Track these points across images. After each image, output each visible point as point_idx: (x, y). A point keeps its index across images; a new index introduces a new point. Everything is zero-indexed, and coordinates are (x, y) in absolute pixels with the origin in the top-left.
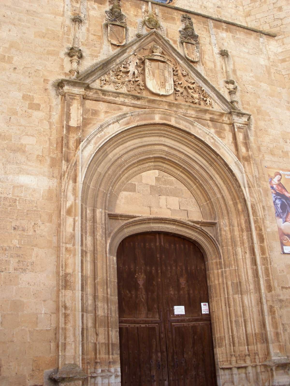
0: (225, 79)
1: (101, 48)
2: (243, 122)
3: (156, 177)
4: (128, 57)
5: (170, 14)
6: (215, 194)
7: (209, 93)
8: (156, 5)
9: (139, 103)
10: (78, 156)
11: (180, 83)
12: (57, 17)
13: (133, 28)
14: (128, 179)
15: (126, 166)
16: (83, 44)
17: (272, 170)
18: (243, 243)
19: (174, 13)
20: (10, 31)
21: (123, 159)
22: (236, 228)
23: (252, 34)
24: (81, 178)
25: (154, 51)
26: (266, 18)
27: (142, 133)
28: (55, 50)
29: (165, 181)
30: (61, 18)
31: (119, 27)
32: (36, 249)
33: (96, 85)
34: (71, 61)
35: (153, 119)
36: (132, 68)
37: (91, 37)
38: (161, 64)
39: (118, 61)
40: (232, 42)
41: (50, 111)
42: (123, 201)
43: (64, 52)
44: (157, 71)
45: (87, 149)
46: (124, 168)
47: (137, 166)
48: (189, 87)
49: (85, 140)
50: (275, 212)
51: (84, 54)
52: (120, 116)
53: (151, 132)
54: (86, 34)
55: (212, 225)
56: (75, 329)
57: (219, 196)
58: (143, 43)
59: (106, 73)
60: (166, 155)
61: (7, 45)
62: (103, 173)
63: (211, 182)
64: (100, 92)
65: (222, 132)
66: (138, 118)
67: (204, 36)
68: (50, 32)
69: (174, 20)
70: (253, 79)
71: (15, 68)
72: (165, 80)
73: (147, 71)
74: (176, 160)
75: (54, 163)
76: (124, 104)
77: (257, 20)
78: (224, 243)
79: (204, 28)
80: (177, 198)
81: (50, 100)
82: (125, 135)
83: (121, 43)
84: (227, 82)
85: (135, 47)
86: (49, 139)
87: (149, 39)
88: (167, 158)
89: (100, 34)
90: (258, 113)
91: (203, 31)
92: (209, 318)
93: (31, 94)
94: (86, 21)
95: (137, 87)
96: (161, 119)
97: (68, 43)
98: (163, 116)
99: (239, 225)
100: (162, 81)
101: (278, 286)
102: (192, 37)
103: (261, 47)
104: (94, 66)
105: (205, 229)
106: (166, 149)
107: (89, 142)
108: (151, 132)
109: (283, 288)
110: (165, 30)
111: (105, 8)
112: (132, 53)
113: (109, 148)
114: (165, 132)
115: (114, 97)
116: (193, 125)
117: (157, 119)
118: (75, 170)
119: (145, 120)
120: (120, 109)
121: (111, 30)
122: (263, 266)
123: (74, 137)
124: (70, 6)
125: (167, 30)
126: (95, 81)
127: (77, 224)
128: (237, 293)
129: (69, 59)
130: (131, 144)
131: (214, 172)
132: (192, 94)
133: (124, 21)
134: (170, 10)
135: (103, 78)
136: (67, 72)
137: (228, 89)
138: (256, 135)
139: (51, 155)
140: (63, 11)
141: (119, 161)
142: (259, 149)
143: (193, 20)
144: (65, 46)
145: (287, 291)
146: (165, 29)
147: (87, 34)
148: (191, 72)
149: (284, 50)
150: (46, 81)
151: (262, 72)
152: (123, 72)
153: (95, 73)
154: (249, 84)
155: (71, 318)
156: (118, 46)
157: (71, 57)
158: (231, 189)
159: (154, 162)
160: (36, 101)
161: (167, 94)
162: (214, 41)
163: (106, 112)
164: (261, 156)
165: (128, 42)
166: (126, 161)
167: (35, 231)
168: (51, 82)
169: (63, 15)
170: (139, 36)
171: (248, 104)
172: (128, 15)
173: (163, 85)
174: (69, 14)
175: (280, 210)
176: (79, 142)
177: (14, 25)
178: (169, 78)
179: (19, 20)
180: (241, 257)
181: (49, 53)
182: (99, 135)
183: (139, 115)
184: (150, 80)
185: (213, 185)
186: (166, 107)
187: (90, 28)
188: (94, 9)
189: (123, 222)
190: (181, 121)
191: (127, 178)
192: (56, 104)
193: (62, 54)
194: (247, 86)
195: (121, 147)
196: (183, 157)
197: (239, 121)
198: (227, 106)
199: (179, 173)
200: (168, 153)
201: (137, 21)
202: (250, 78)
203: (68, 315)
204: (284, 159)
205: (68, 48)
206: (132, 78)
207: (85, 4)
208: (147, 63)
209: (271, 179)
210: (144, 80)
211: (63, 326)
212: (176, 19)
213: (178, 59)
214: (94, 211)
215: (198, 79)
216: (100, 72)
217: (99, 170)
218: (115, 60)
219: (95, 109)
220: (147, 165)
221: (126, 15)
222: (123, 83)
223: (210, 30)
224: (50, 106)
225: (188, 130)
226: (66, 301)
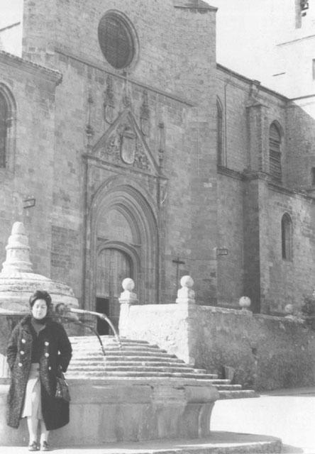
18: (152, 260)
36: (117, 143)
55: (140, 247)
76: (111, 170)
105: (136, 249)
197: (163, 183)
210: (121, 153)
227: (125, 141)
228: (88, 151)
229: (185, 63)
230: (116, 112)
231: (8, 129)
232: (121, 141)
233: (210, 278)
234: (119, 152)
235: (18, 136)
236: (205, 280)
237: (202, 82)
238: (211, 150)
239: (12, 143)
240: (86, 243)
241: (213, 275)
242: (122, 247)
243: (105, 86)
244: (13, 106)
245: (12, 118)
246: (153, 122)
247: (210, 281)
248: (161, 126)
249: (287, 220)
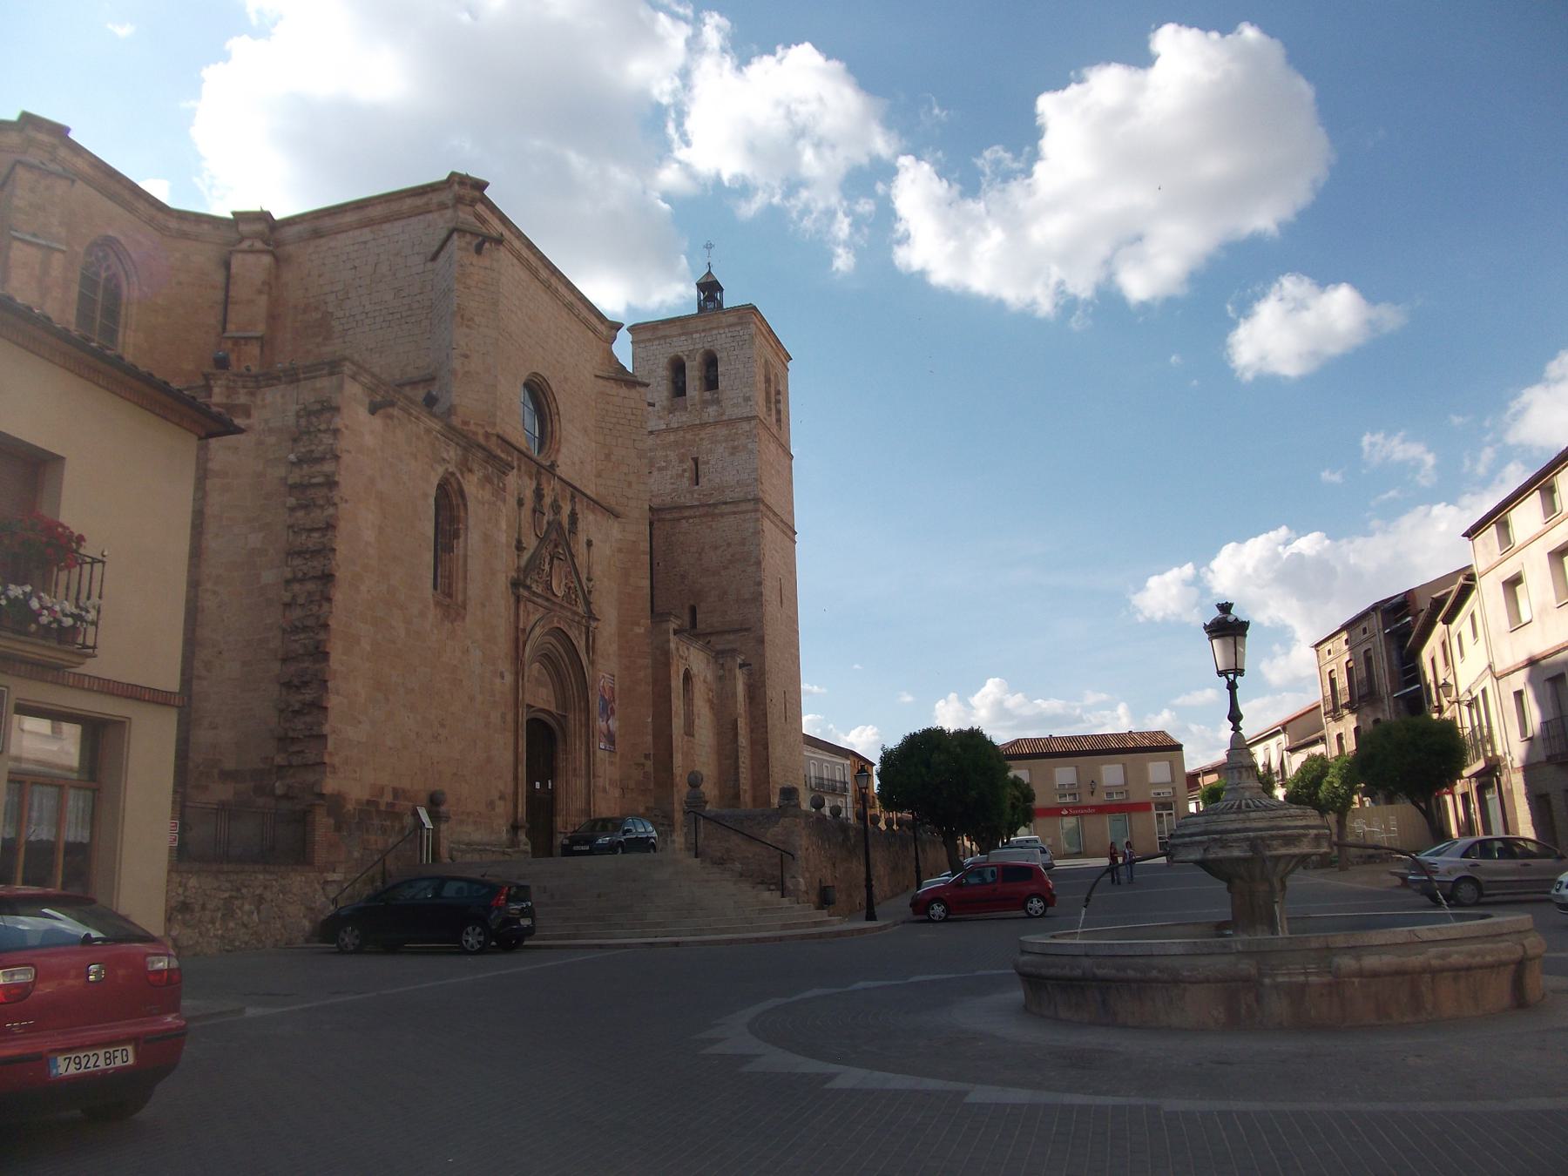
18: (580, 736)
22: (577, 722)
24: (526, 678)
36: (547, 567)
55: (565, 716)
72: (561, 582)
92: (552, 792)
99: (580, 720)
196: (557, 654)
197: (594, 624)
200: (552, 652)
209: (600, 681)
227: (555, 561)
228: (518, 576)
229: (608, 456)
230: (546, 518)
231: (455, 541)
234: (549, 579)
235: (469, 553)
236: (638, 764)
237: (630, 484)
239: (461, 562)
240: (518, 711)
241: (647, 756)
242: (546, 716)
243: (534, 486)
244: (462, 507)
245: (461, 526)
246: (582, 538)
247: (643, 765)
248: (589, 544)
249: (687, 677)
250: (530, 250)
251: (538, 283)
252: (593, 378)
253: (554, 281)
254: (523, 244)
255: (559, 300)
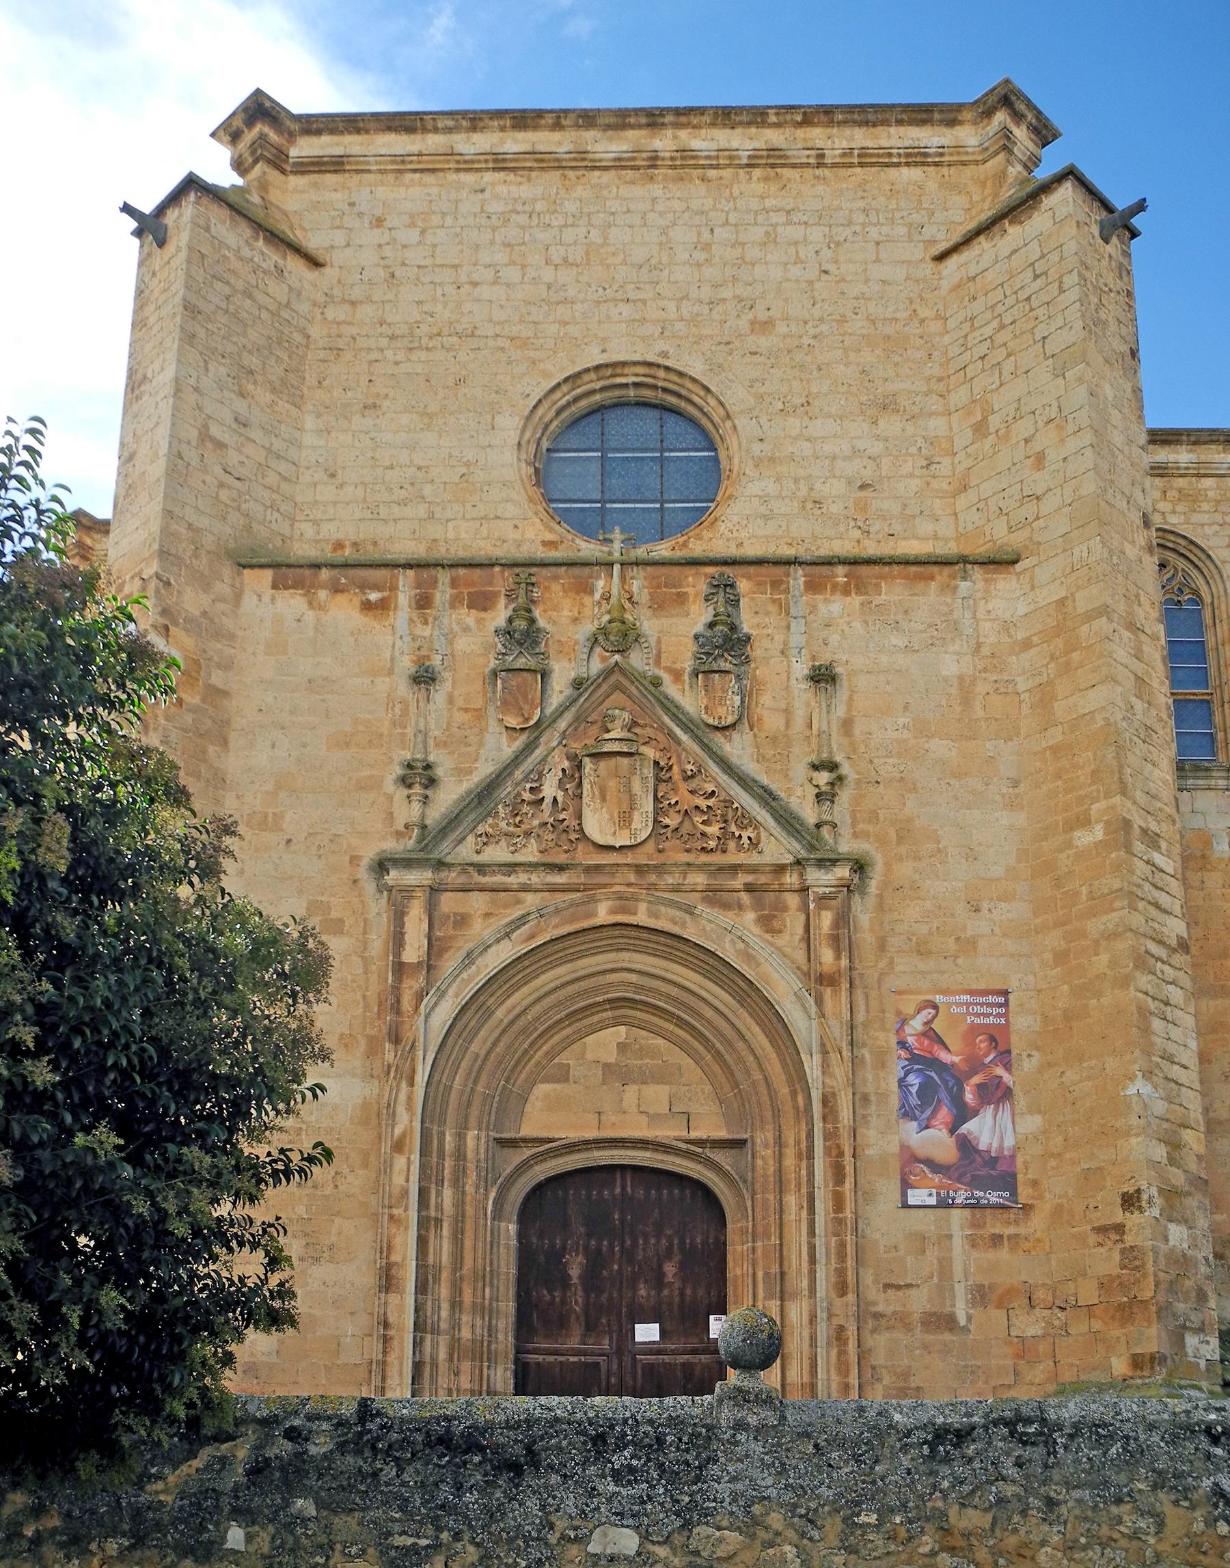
0: (813, 758)
1: (481, 744)
2: (835, 883)
3: (618, 1044)
4: (547, 756)
5: (675, 587)
6: (748, 1072)
7: (754, 814)
8: (635, 568)
9: (560, 879)
10: (417, 1029)
11: (673, 802)
12: (377, 681)
13: (566, 664)
14: (552, 1055)
15: (541, 1029)
16: (437, 745)
17: (912, 997)
18: (799, 1185)
19: (686, 577)
20: (273, 746)
21: (529, 1017)
23: (932, 578)
25: (610, 726)
26: (1001, 495)
27: (572, 951)
28: (372, 776)
29: (641, 1049)
30: (387, 679)
31: (525, 674)
32: (338, 1220)
33: (467, 851)
34: (409, 797)
35: (593, 914)
36: (550, 789)
37: (460, 717)
38: (625, 761)
39: (518, 774)
40: (857, 625)
41: (365, 933)
42: (539, 1104)
43: (394, 776)
44: (612, 784)
45: (438, 1010)
46: (535, 1035)
47: (569, 1025)
48: (697, 807)
49: (432, 993)
50: (897, 1107)
51: (439, 772)
52: (512, 922)
53: (592, 945)
54: (445, 712)
55: (739, 1144)
56: (401, 1364)
57: (757, 1076)
58: (587, 705)
59: (489, 815)
60: (635, 992)
61: (269, 787)
62: (483, 1053)
63: (740, 1045)
64: (470, 869)
65: (775, 916)
66: (555, 921)
67: (770, 631)
68: (361, 728)
69: (683, 603)
70: (906, 735)
71: (289, 841)
73: (586, 786)
74: (660, 1000)
75: (373, 1050)
76: (526, 888)
77: (981, 505)
78: (758, 1187)
79: (774, 601)
80: (667, 1088)
81: (363, 906)
82: (526, 963)
83: (527, 720)
84: (815, 767)
85: (562, 724)
86: (364, 997)
87: (605, 687)
88: (638, 997)
89: (479, 704)
90: (900, 840)
91: (768, 613)
93: (323, 899)
94: (446, 675)
95: (564, 836)
96: (613, 912)
97: (404, 749)
98: (617, 903)
100: (625, 807)
101: (876, 1282)
102: (728, 646)
103: (957, 614)
104: (462, 799)
106: (633, 978)
107: (442, 994)
108: (592, 945)
109: (887, 1286)
110: (653, 644)
111: (493, 619)
112: (555, 744)
113: (493, 999)
114: (626, 941)
115: (504, 875)
116: (692, 914)
117: (603, 914)
118: (413, 1059)
119: (572, 922)
120: (518, 902)
121: (504, 688)
122: (834, 1239)
123: (411, 987)
124: (407, 639)
125: (659, 642)
126: (464, 839)
127: (412, 1168)
128: (770, 1296)
129: (406, 792)
130: (547, 979)
131: (749, 1019)
132: (702, 827)
133: (542, 648)
134: (675, 570)
135: (480, 829)
136: (402, 828)
137: (817, 786)
138: (881, 907)
139: (369, 1031)
140: (392, 659)
141: (522, 1022)
142: (882, 945)
143: (743, 585)
144: (397, 759)
145: (900, 1293)
146: (653, 641)
147: (449, 710)
148: (710, 762)
149: (1032, 607)
150: (354, 860)
151: (944, 702)
152: (529, 803)
153: (462, 821)
154: (890, 754)
155: (395, 1343)
156: (522, 729)
157: (410, 786)
158: (785, 1060)
159: (611, 1009)
160: (334, 914)
161: (633, 842)
162: (797, 639)
163: (487, 915)
164: (882, 964)
165: (548, 711)
166: (536, 1019)
167: (336, 1186)
168: (365, 862)
169: (391, 671)
170: (578, 684)
171: (874, 817)
172: (555, 623)
173: (625, 819)
174: (406, 664)
175: (914, 1101)
176: (420, 996)
177: (283, 728)
178: (644, 796)
179: (292, 713)
180: (793, 1217)
181: (361, 787)
182: (465, 975)
183: (557, 911)
184: (595, 812)
185: (745, 1053)
186: (632, 878)
187: (456, 693)
188: (466, 629)
189: (527, 1153)
190: (663, 909)
191: (548, 1053)
192: (378, 914)
193: (389, 785)
194: (882, 761)
195: (525, 990)
198: (800, 842)
199: (672, 1027)
201: (577, 637)
202: (896, 735)
203: (392, 1338)
204: (960, 961)
205: (401, 764)
206: (550, 816)
207: (446, 621)
208: (588, 764)
209: (904, 1022)
210: (579, 816)
211: (380, 1357)
212: (691, 599)
213: (678, 731)
214: (460, 1137)
215: (725, 777)
216: (472, 816)
217: (474, 1047)
218: (511, 774)
219: (461, 910)
220: (595, 1018)
221: (549, 628)
222: (528, 834)
223: (792, 604)
224: (365, 920)
225: (676, 930)
226: (389, 1314)
229: (980, 429)
232: (573, 775)
233: (1119, 1216)
236: (1101, 1230)
238: (1092, 694)
247: (1120, 1228)
250: (536, 127)
251: (608, 177)
252: (930, 266)
253: (664, 142)
254: (503, 129)
255: (717, 167)
